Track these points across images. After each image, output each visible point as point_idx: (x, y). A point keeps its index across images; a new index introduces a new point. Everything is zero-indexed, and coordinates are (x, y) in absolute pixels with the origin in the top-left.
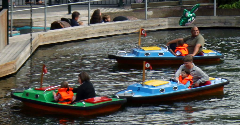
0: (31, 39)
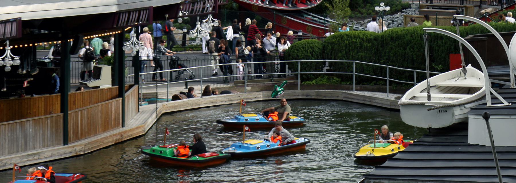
0: (157, 108)
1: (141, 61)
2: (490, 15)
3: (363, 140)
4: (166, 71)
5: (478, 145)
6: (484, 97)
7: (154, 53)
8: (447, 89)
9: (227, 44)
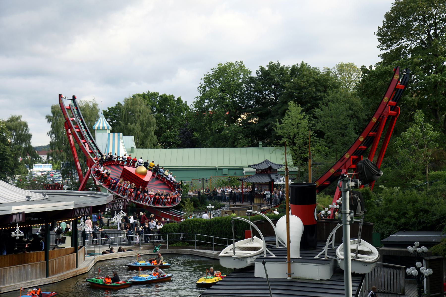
0: (94, 258)
1: (86, 234)
2: (266, 210)
3: (200, 275)
4: (99, 239)
5: (260, 277)
6: (263, 253)
7: (93, 230)
8: (247, 249)
9: (131, 225)
